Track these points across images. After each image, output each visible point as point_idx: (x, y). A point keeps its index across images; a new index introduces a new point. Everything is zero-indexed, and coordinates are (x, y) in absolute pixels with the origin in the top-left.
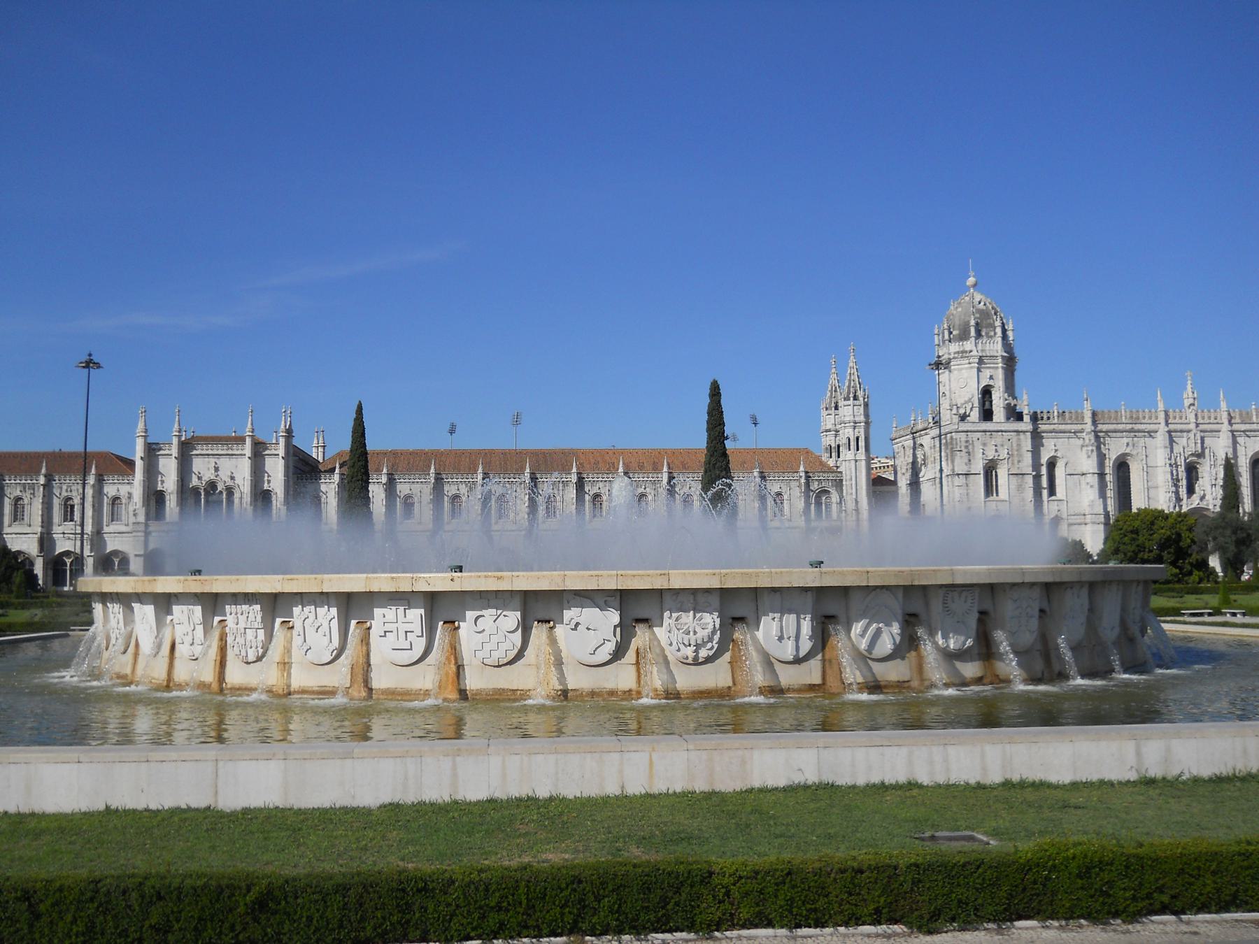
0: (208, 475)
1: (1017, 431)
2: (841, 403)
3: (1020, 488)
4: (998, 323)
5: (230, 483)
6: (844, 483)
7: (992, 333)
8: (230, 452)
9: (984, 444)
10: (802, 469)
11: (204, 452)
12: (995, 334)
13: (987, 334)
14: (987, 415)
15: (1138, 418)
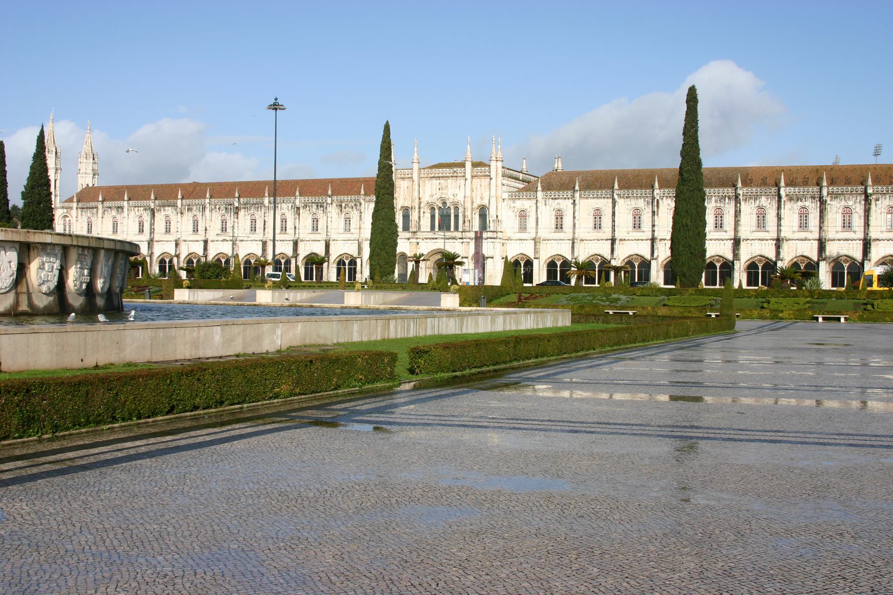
8: (455, 174)
11: (437, 175)
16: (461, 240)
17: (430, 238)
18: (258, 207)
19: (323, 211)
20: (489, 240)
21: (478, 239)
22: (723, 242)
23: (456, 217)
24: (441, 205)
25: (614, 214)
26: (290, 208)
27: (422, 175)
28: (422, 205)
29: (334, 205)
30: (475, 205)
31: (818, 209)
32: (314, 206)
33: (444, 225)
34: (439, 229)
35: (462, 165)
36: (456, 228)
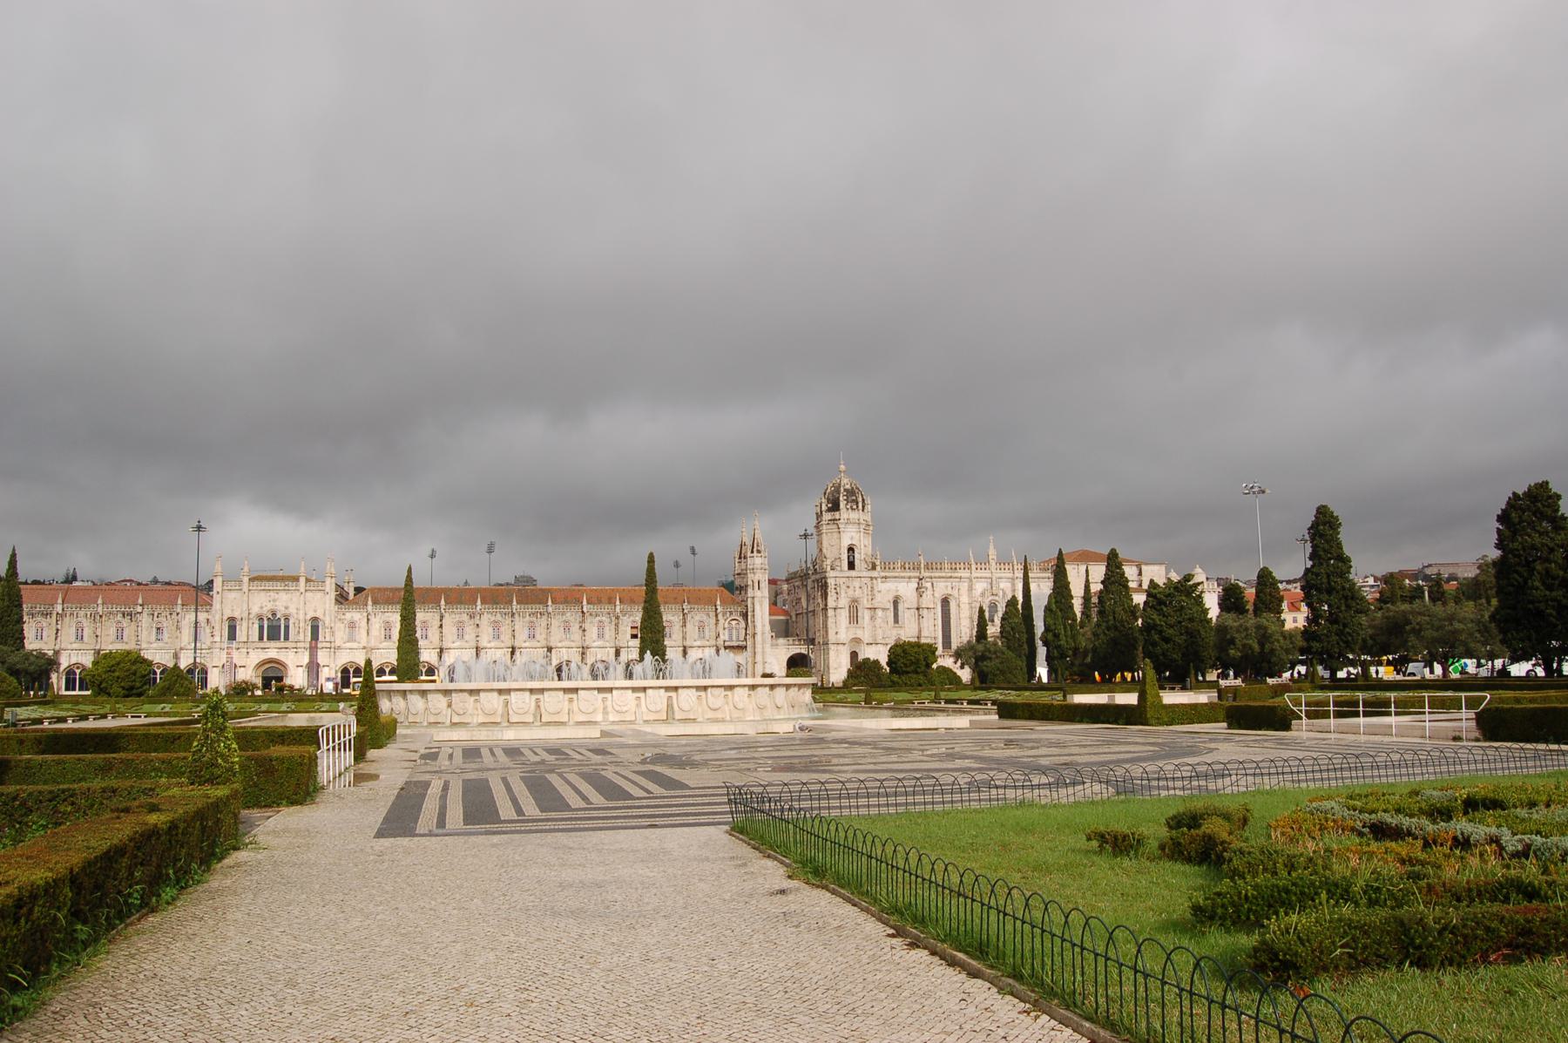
0: (270, 606)
1: (871, 577)
2: (749, 554)
3: (872, 618)
4: (860, 499)
5: (287, 612)
6: (749, 614)
7: (855, 507)
8: (286, 588)
9: (848, 587)
10: (718, 603)
11: (267, 588)
12: (857, 507)
13: (851, 507)
14: (851, 566)
15: (956, 569)
16: (295, 650)
17: (262, 648)
18: (47, 614)
19: (131, 619)
20: (324, 650)
21: (313, 650)
22: (606, 650)
23: (287, 627)
24: (270, 616)
25: (441, 626)
26: (89, 616)
27: (251, 588)
28: (251, 616)
29: (145, 614)
30: (308, 617)
31: (613, 623)
32: (120, 615)
33: (274, 634)
34: (268, 639)
35: (296, 579)
36: (287, 638)
